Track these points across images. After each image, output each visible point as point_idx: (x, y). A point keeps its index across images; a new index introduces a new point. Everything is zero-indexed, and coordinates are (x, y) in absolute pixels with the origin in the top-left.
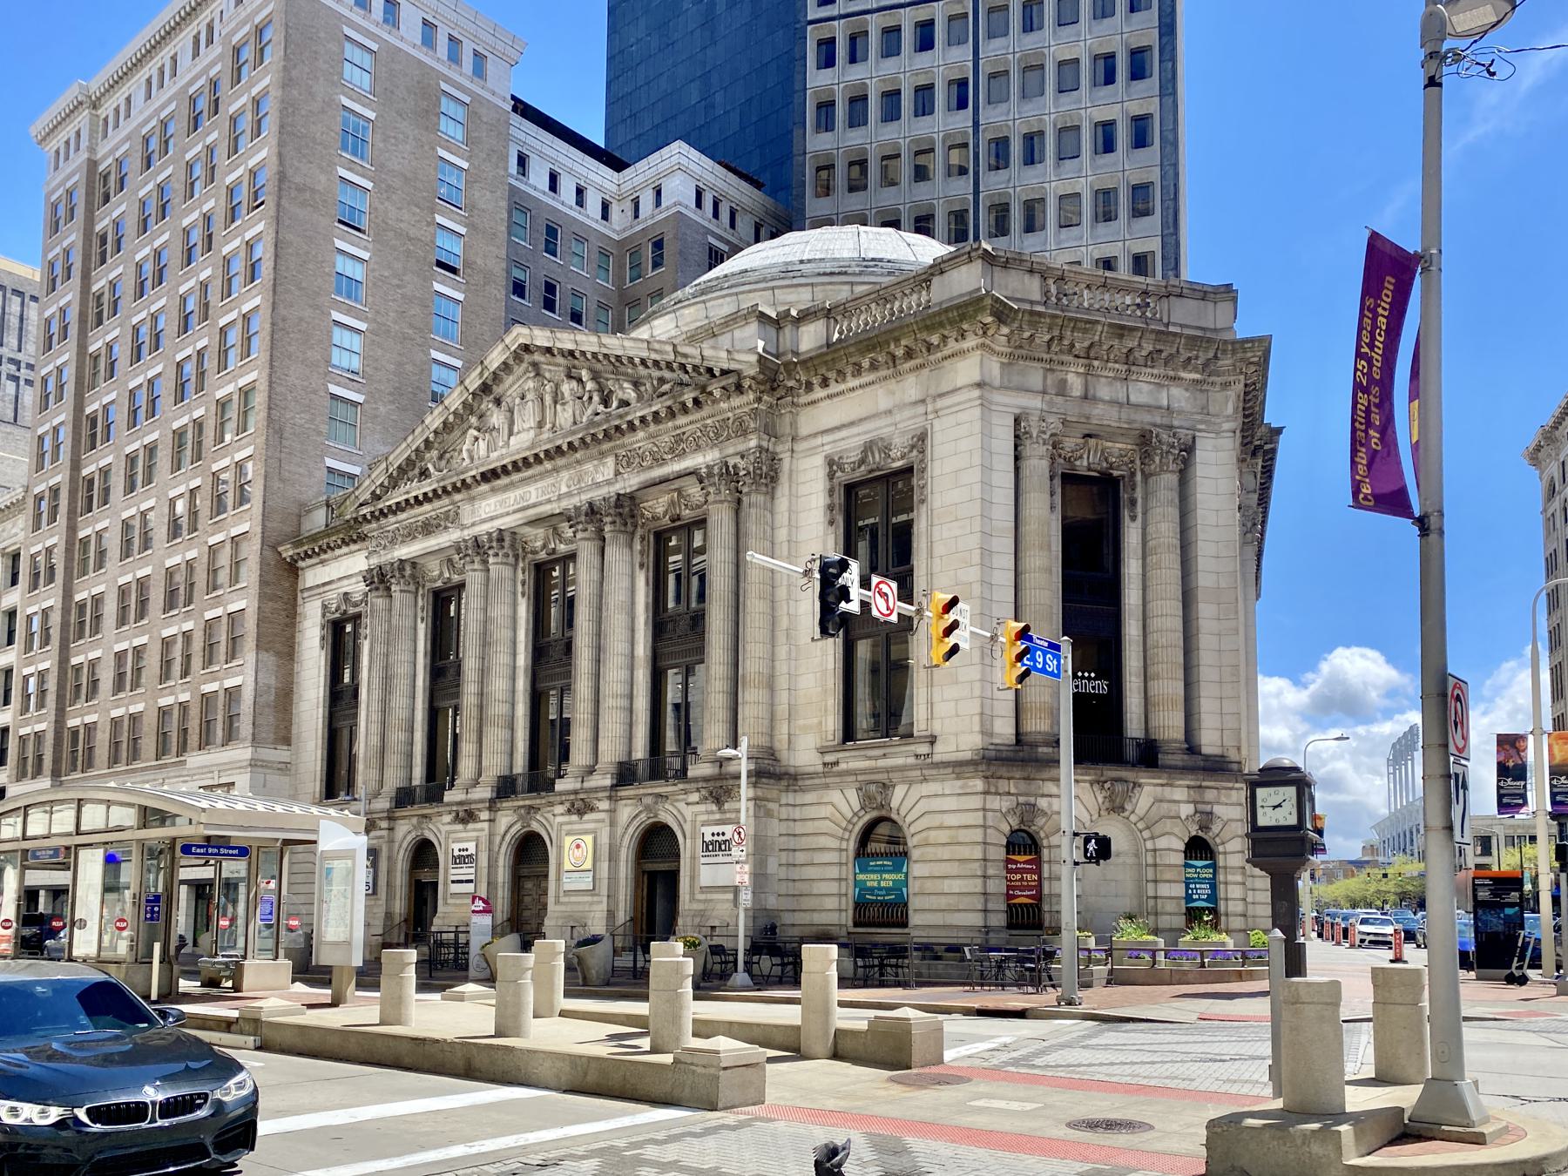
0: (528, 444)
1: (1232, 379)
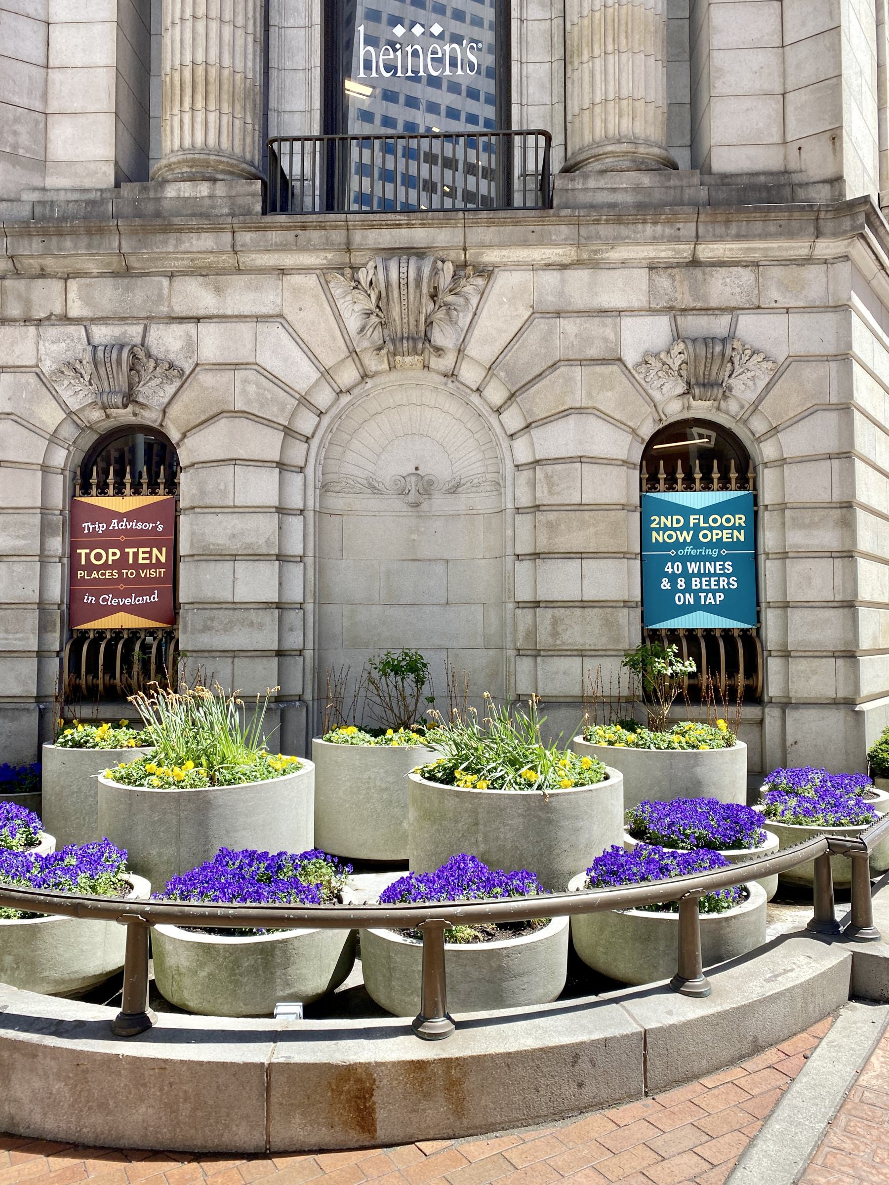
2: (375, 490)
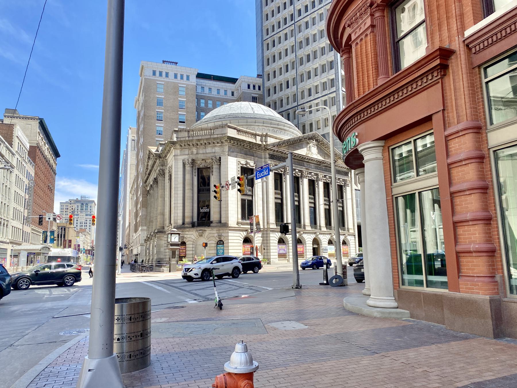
2: (200, 245)
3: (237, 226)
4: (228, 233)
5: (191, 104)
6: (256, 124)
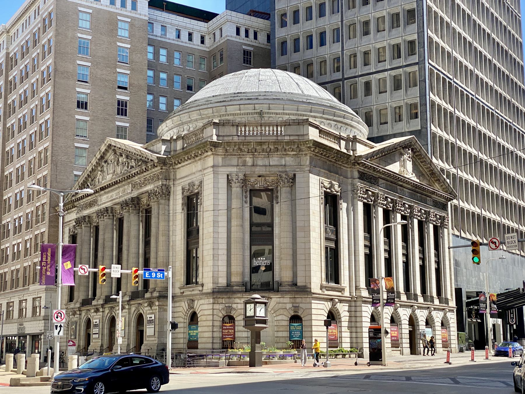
0: (110, 179)
1: (307, 152)
3: (320, 292)
4: (311, 303)
5: (139, 55)
6: (312, 114)
